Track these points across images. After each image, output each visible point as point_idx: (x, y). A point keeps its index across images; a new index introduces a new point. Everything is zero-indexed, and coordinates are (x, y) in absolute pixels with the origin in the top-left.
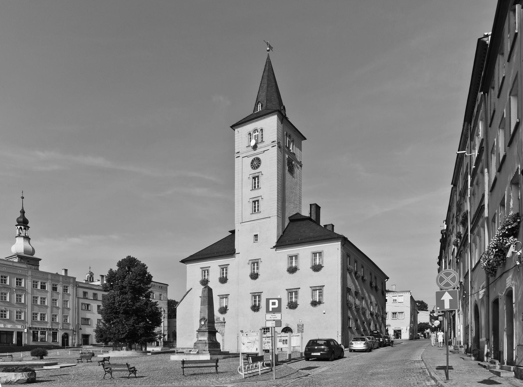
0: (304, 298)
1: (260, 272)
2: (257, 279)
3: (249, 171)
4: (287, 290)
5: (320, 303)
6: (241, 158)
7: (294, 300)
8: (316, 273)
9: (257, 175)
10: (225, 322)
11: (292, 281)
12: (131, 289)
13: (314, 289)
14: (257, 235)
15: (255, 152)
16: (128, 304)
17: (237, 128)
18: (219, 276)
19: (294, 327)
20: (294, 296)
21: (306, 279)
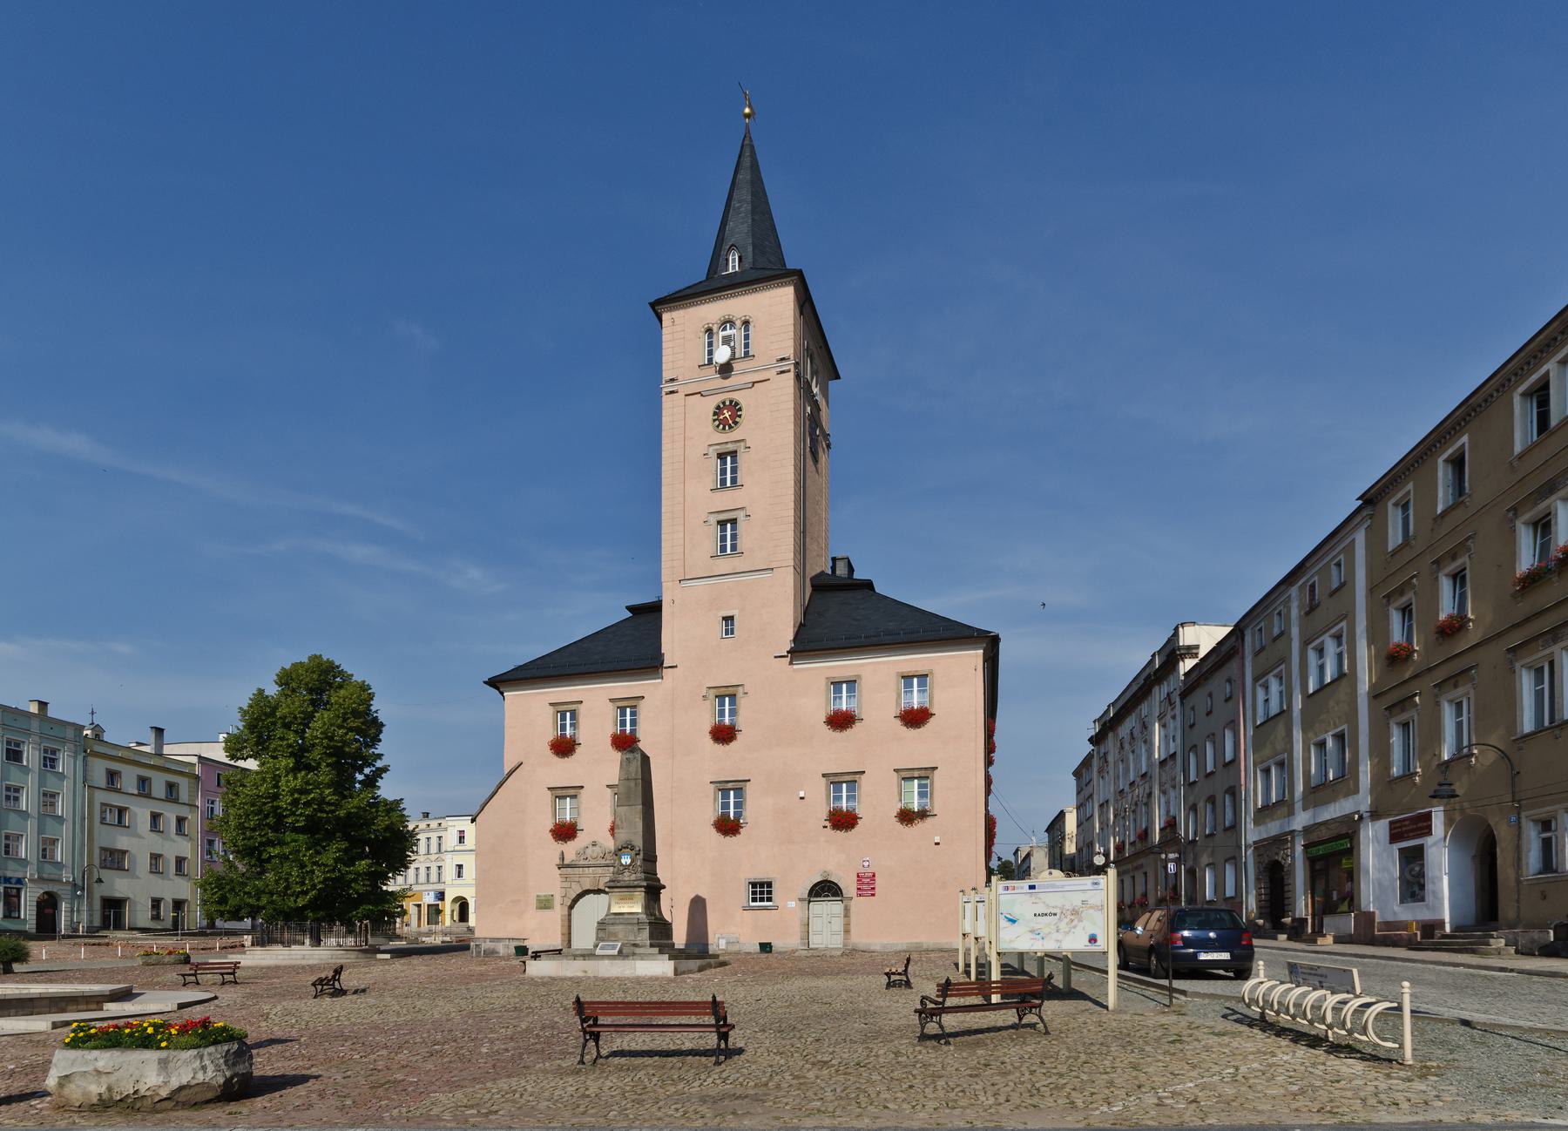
1: (741, 723)
2: (733, 744)
3: (706, 436)
15: (727, 383)
19: (848, 885)
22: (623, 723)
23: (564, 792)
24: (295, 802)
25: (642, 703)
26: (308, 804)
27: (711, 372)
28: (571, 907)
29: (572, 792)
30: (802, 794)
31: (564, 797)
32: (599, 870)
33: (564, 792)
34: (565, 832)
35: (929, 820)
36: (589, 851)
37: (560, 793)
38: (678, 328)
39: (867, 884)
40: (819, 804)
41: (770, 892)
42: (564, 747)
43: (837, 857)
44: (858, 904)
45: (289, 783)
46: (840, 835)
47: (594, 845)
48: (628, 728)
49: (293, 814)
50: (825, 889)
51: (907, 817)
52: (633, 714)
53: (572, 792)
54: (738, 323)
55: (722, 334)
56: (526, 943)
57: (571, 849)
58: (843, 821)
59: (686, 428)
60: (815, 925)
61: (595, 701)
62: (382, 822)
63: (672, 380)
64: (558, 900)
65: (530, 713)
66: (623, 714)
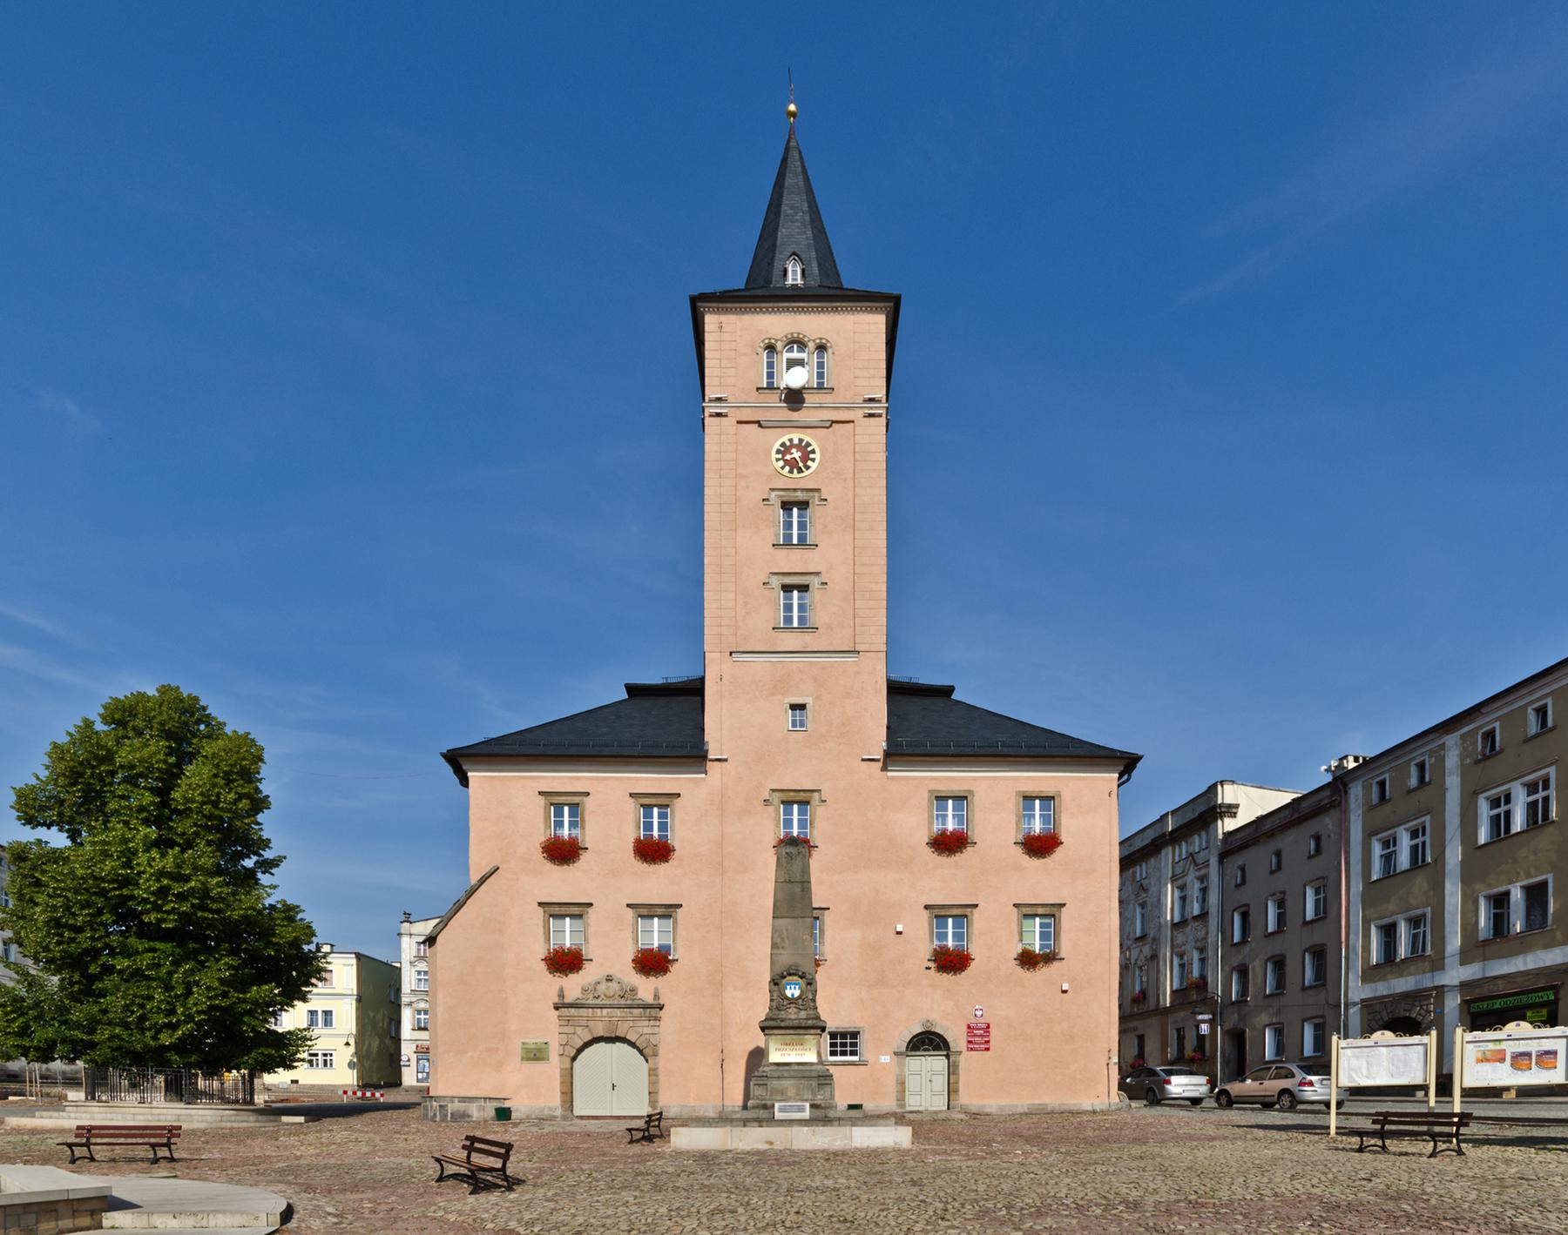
0: (995, 939)
4: (926, 907)
5: (1050, 958)
6: (729, 423)
7: (950, 943)
8: (1036, 863)
9: (800, 496)
10: (661, 1008)
11: (947, 880)
12: (208, 829)
13: (1027, 912)
14: (802, 707)
15: (795, 416)
16: (205, 894)
17: (719, 311)
18: (630, 833)
19: (956, 1037)
20: (950, 930)
21: (996, 879)
22: (648, 826)
23: (564, 910)
24: (163, 892)
25: (678, 803)
26: (181, 897)
27: (774, 399)
28: (574, 1059)
29: (576, 910)
30: (900, 928)
31: (563, 916)
32: (618, 1012)
33: (564, 910)
34: (565, 962)
35: (1056, 964)
36: (602, 987)
37: (557, 910)
38: (727, 337)
39: (980, 1036)
40: (920, 940)
41: (854, 1045)
42: (562, 852)
43: (943, 1004)
44: (969, 1061)
45: (151, 863)
46: (947, 978)
47: (609, 979)
48: (656, 833)
49: (158, 908)
50: (928, 1041)
51: (1028, 960)
52: (662, 816)
53: (576, 910)
54: (811, 345)
55: (786, 355)
56: (507, 1104)
57: (573, 985)
58: (951, 962)
59: (739, 464)
60: (912, 1084)
61: (610, 796)
62: (285, 934)
63: (719, 399)
64: (554, 1051)
65: (508, 802)
66: (648, 815)
